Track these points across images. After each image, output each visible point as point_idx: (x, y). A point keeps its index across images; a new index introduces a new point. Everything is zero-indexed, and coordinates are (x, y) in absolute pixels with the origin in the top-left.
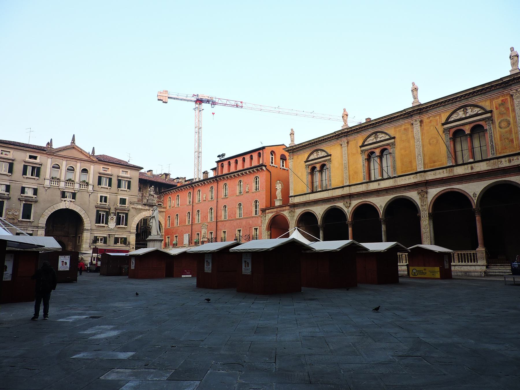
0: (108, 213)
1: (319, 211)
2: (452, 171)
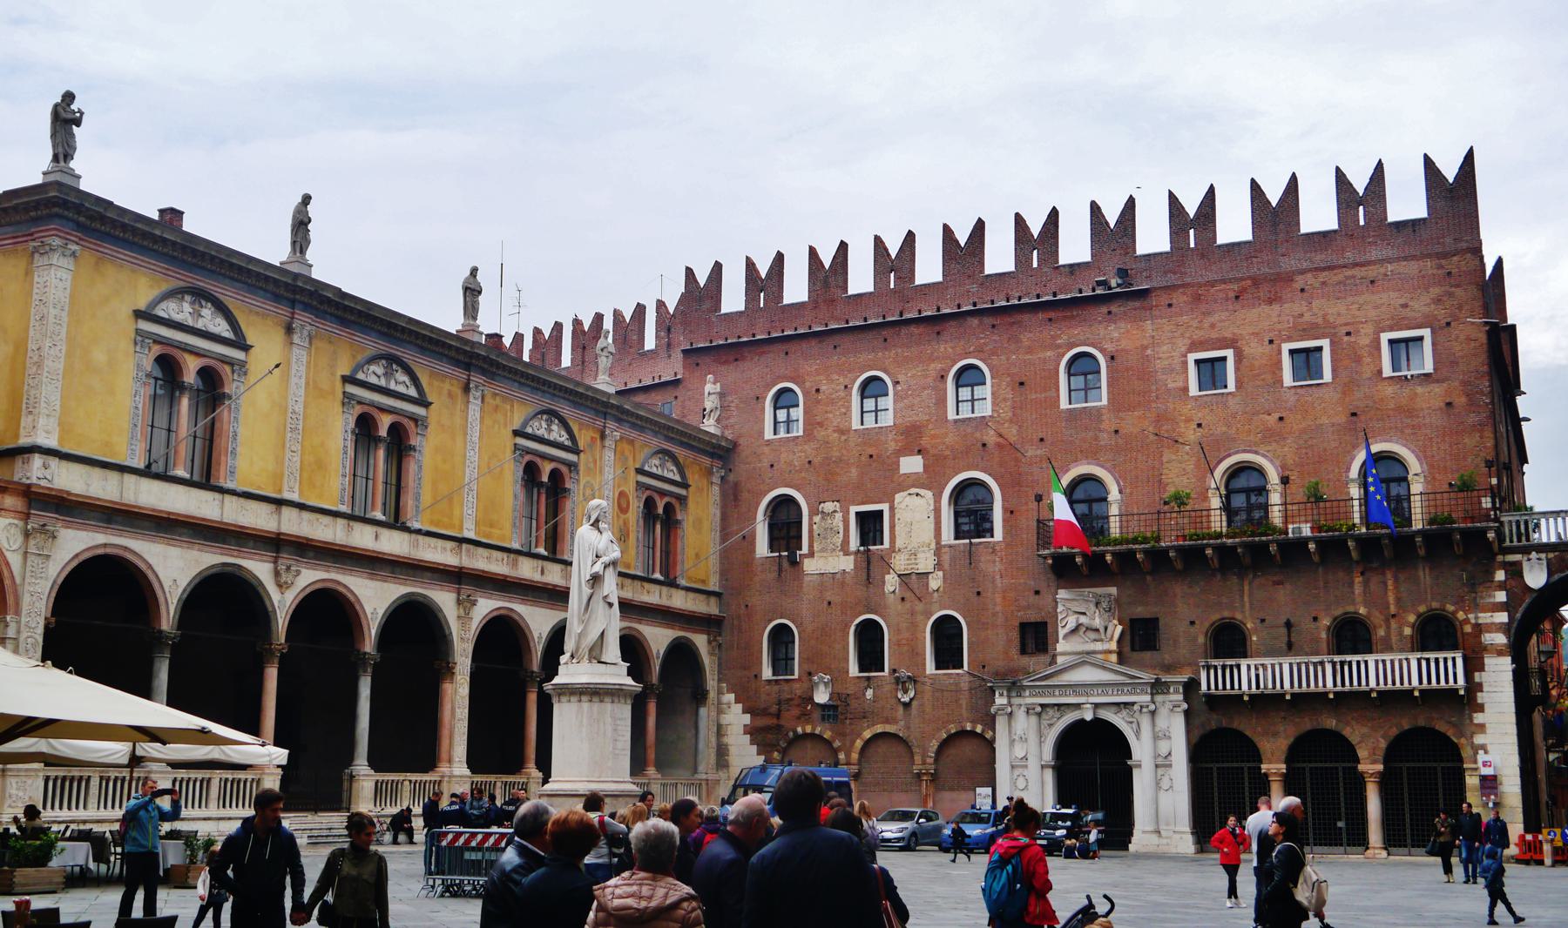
1: (174, 569)
2: (515, 565)
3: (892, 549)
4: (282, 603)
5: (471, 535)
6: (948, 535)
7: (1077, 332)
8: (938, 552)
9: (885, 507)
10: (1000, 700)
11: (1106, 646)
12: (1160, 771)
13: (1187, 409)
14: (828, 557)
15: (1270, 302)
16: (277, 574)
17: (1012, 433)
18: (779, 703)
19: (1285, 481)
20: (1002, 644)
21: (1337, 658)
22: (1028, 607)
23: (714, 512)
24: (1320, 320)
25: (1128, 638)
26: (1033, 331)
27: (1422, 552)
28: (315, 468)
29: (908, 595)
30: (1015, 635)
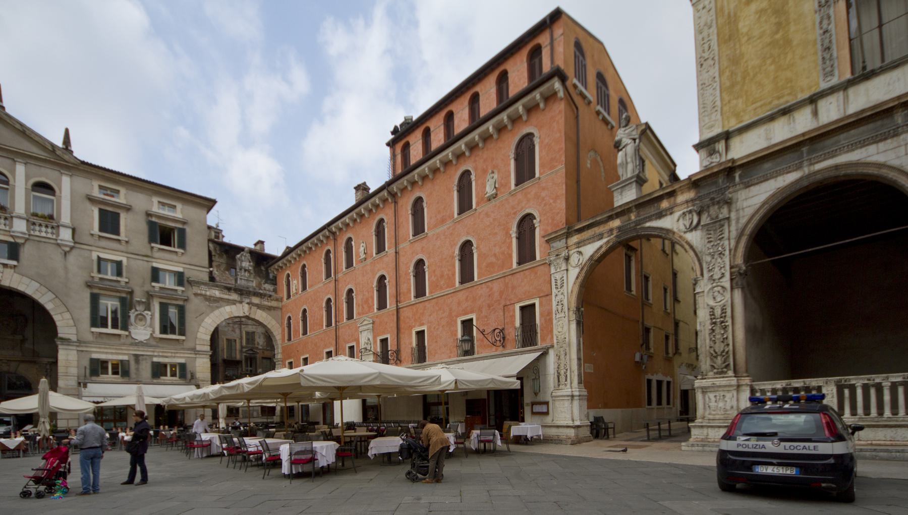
0: (127, 303)
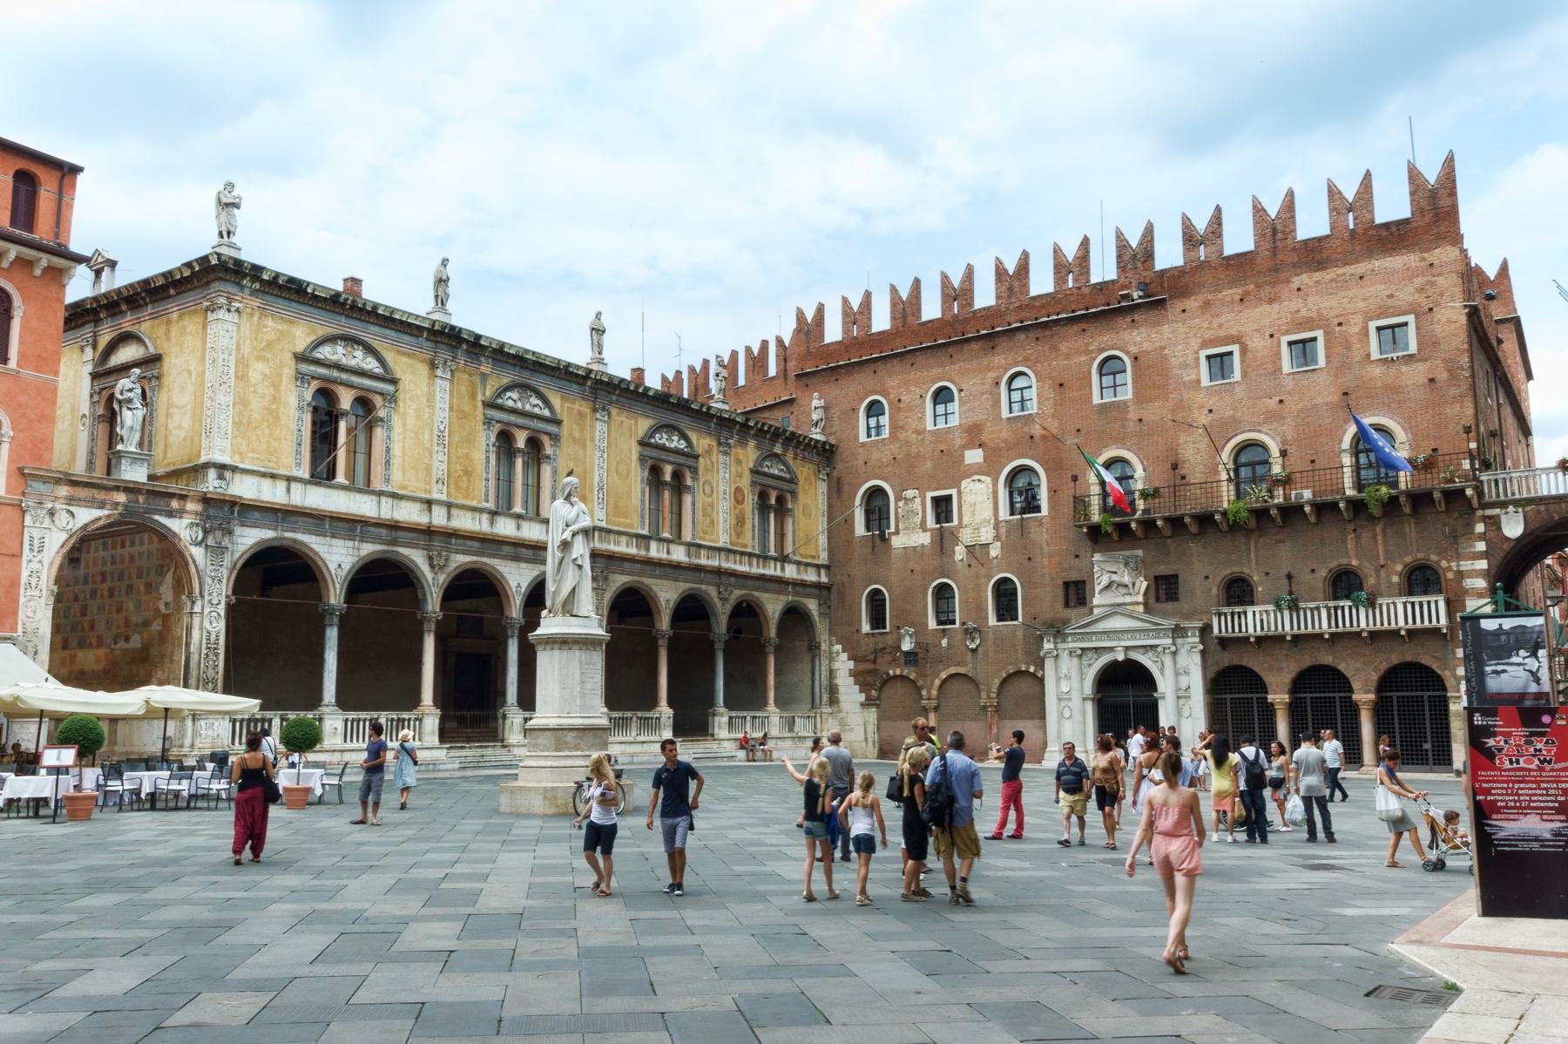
3: (960, 525)
4: (434, 584)
5: (603, 524)
6: (1004, 514)
7: (1106, 338)
8: (996, 527)
9: (953, 492)
10: (1048, 646)
11: (1133, 599)
12: (1182, 702)
13: (1199, 398)
14: (911, 534)
15: (1271, 301)
16: (430, 558)
17: (1054, 426)
18: (875, 651)
19: (1284, 454)
20: (1049, 602)
21: (1331, 604)
22: (1070, 568)
23: (822, 505)
24: (1314, 315)
25: (1152, 591)
26: (1071, 342)
27: (1407, 510)
28: (460, 475)
29: (974, 562)
30: (1060, 593)
